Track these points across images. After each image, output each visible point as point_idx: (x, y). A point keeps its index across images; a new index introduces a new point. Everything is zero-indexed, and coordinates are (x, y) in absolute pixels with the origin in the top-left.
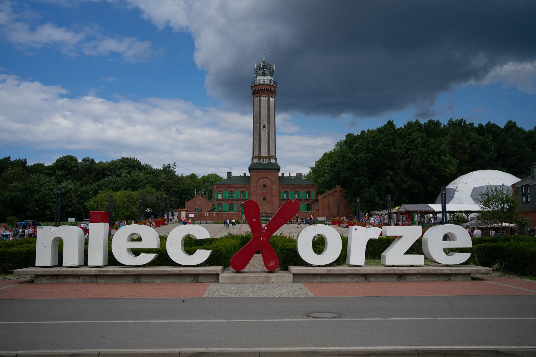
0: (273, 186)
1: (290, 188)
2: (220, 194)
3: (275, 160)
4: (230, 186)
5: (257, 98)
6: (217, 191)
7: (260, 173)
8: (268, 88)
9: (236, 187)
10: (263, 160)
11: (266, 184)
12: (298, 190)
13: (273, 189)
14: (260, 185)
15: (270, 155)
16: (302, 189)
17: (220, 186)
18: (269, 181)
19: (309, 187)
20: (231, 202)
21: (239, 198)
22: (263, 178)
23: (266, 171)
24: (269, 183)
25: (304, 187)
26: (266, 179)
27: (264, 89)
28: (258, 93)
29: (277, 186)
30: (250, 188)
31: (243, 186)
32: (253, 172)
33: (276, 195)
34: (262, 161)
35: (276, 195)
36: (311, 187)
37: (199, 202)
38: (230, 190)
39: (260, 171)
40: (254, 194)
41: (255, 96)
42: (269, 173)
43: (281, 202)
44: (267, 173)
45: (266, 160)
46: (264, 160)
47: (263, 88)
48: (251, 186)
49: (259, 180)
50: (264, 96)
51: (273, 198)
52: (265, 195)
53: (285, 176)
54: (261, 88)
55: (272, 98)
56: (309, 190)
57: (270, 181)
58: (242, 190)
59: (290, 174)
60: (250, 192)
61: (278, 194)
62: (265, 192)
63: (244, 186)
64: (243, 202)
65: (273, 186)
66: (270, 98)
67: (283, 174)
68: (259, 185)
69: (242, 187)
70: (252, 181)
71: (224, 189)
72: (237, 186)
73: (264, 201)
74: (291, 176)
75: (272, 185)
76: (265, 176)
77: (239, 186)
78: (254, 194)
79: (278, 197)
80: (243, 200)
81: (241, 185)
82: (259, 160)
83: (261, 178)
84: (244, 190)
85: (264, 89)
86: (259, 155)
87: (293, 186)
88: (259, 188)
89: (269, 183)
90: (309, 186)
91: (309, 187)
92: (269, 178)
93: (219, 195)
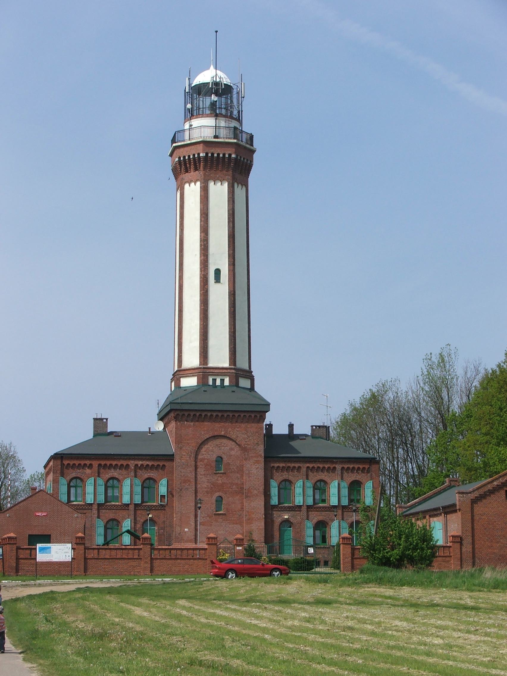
2: (75, 487)
4: (108, 463)
5: (193, 184)
6: (69, 478)
8: (229, 152)
9: (127, 465)
10: (214, 380)
14: (206, 461)
15: (235, 364)
17: (77, 462)
18: (232, 449)
20: (111, 515)
24: (233, 453)
26: (224, 441)
27: (215, 155)
28: (196, 169)
29: (257, 462)
31: (150, 463)
33: (255, 492)
34: (211, 383)
35: (255, 492)
37: (42, 512)
38: (108, 476)
41: (187, 176)
46: (218, 383)
47: (213, 154)
50: (218, 179)
53: (275, 431)
54: (207, 154)
55: (240, 186)
57: (237, 448)
58: (146, 476)
59: (291, 426)
61: (262, 488)
62: (220, 482)
63: (156, 463)
66: (236, 185)
67: (270, 426)
69: (148, 465)
71: (88, 471)
72: (132, 462)
74: (296, 432)
76: (223, 433)
80: (150, 509)
82: (203, 381)
83: (208, 437)
84: (152, 474)
85: (215, 155)
86: (200, 365)
87: (308, 465)
88: (201, 471)
89: (233, 453)
92: (233, 437)
93: (73, 490)
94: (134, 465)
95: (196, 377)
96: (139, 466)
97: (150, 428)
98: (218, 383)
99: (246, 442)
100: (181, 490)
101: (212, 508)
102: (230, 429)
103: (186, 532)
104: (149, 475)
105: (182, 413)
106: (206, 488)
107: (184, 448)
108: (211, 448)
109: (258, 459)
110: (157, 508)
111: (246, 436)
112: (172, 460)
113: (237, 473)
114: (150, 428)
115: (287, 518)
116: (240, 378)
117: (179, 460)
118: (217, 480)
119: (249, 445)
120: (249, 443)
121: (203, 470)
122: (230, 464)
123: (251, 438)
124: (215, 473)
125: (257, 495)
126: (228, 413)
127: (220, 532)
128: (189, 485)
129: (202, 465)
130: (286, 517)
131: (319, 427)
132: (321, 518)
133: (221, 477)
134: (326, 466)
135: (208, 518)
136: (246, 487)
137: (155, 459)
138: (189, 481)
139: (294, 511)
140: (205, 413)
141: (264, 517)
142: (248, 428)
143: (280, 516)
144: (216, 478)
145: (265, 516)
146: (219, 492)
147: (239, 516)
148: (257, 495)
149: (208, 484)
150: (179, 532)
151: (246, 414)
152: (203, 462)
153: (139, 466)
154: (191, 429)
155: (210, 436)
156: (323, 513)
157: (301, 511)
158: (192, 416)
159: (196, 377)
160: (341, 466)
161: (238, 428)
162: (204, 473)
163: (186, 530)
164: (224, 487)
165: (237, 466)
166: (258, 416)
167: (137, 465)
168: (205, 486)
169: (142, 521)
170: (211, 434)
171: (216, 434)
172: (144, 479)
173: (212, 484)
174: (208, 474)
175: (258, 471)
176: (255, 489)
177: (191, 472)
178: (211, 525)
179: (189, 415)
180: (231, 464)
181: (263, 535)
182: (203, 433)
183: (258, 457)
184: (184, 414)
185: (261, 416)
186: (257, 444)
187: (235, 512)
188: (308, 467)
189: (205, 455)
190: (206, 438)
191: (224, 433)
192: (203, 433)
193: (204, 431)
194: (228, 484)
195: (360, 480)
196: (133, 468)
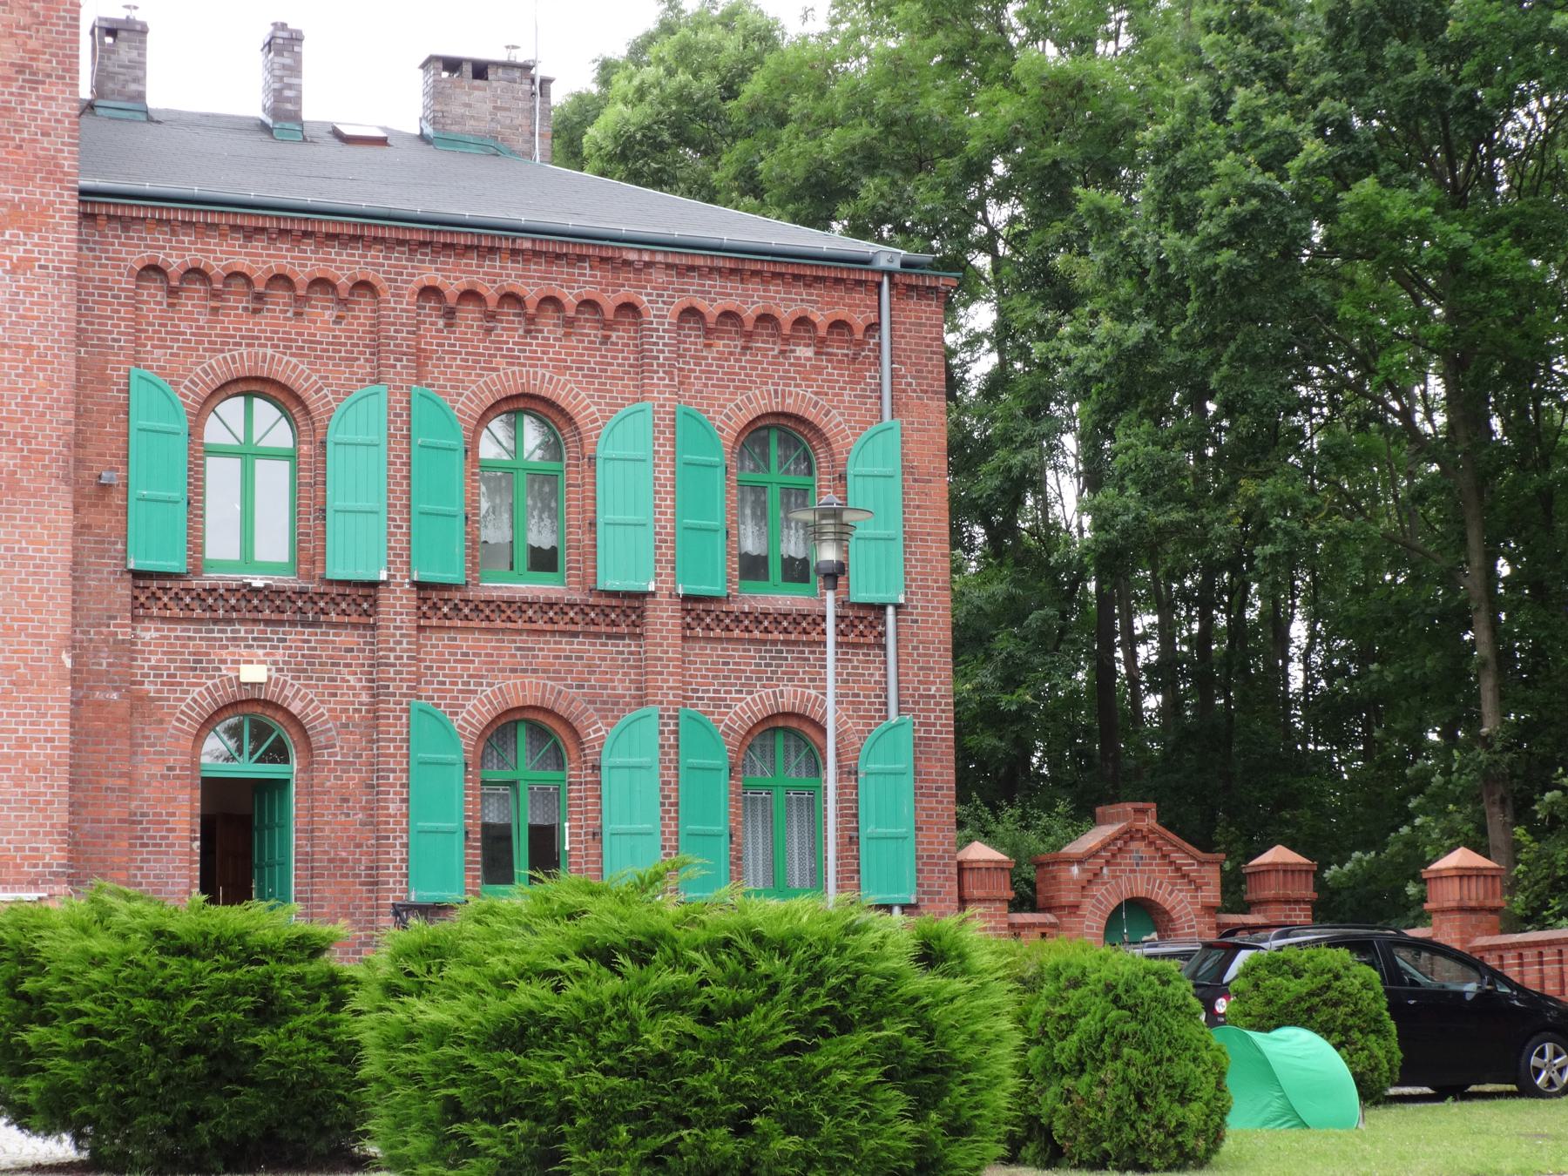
1: (363, 309)
12: (543, 381)
16: (642, 363)
19: (802, 322)
25: (691, 314)
36: (839, 325)
43: (128, 649)
56: (799, 399)
61: (54, 428)
79: (59, 511)
87: (430, 272)
90: (787, 303)
91: (802, 322)
109: (36, 192)
130: (253, 673)
131: (481, 70)
132: (524, 690)
134: (570, 297)
139: (315, 624)
141: (68, 663)
145: (74, 658)
156: (547, 649)
157: (373, 627)
160: (680, 302)
175: (29, 291)
181: (61, 816)
186: (21, 69)
188: (429, 292)
195: (811, 414)
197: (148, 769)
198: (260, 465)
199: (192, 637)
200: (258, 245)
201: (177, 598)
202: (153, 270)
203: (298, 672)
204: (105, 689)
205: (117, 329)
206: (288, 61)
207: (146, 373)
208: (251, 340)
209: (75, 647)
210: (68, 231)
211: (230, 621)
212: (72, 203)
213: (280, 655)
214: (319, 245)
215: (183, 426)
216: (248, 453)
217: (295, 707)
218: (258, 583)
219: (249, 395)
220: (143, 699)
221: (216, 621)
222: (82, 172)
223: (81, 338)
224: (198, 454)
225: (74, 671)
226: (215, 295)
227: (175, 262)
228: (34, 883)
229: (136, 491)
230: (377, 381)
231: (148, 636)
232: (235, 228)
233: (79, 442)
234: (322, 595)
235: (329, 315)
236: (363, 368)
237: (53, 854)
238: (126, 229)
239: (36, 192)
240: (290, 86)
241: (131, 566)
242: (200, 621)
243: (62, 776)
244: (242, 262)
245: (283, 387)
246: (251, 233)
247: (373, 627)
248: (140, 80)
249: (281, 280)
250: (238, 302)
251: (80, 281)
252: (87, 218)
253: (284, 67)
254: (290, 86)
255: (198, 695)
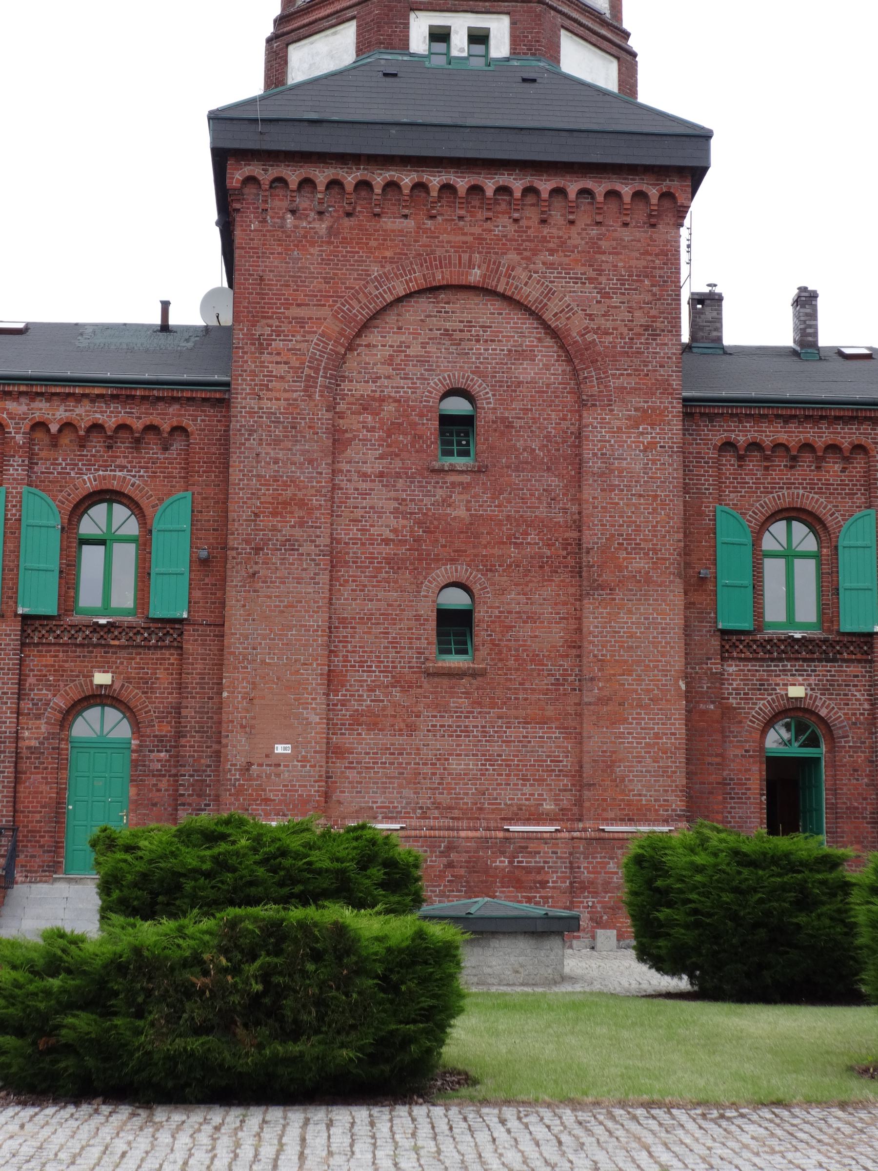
0: (588, 418)
1: (859, 464)
3: (614, 65)
7: (390, 223)
10: (440, 36)
11: (478, 387)
13: (594, 465)
14: (389, 408)
18: (520, 355)
21: (50, 609)
22: (433, 290)
23: (490, 186)
24: (526, 371)
30: (225, 442)
32: (279, 203)
33: (639, 563)
39: (392, 186)
40: (290, 544)
42: (531, 216)
43: (719, 678)
44: (503, 226)
45: (479, 38)
46: (459, 43)
48: (240, 420)
49: (366, 326)
51: (592, 623)
52: (461, 572)
58: (89, 481)
60: (223, 503)
62: (461, 512)
64: (102, 678)
65: (588, 418)
68: (366, 406)
69: (96, 427)
70: (262, 344)
73: (454, 661)
75: (582, 403)
76: (475, 276)
77: (41, 409)
78: (290, 544)
79: (675, 596)
81: (79, 398)
89: (526, 371)
92: (531, 293)
94: (25, 426)
95: (353, 25)
96: (54, 428)
97: (165, 305)
98: (459, 43)
99: (591, 317)
100: (258, 550)
101: (415, 645)
102: (513, 256)
103: (277, 763)
104: (104, 478)
105: (274, 172)
106: (387, 541)
107: (278, 344)
108: (415, 350)
109: (656, 401)
110: (139, 638)
111: (590, 292)
112: (228, 407)
113: (549, 469)
114: (165, 305)
115: (802, 695)
116: (563, 33)
117: (254, 403)
118: (446, 502)
119: (607, 333)
120: (609, 325)
121: (371, 455)
122: (510, 426)
123: (615, 300)
124: (433, 471)
125: (648, 581)
126: (504, 179)
127: (456, 765)
128: (302, 524)
129: (372, 430)
130: (796, 691)
133: (466, 487)
135: (396, 693)
136: (592, 537)
137: (133, 397)
138: (302, 504)
139: (834, 660)
140: (391, 174)
141: (683, 687)
142: (604, 253)
143: (762, 687)
144: (440, 493)
145: (687, 684)
146: (453, 561)
147: (557, 683)
148: (648, 581)
149: (393, 523)
150: (241, 761)
151: (589, 184)
152: (375, 414)
153: (54, 428)
154: (315, 250)
155: (414, 288)
157: (871, 662)
158: (321, 187)
159: (353, 25)
161: (552, 252)
162: (379, 466)
163: (280, 749)
164: (477, 536)
165: (548, 437)
166: (654, 193)
167: (40, 426)
168: (388, 534)
169: (60, 702)
170: (417, 278)
171: (440, 277)
172: (76, 497)
173: (420, 523)
174: (398, 475)
175: (654, 462)
176: (637, 548)
177: (311, 462)
178: (412, 728)
179: (307, 183)
180: (517, 423)
181: (681, 780)
182: (376, 271)
183: (650, 393)
184: (280, 181)
185: (667, 196)
187: (535, 659)
189: (386, 382)
190: (389, 298)
191: (484, 276)
192: (376, 271)
193: (382, 262)
194: (500, 524)
196: (20, 439)
197: (733, 752)
198: (798, 562)
199: (759, 670)
200: (792, 426)
201: (748, 646)
202: (728, 446)
203: (824, 690)
204: (705, 703)
205: (708, 483)
206: (808, 311)
207: (726, 508)
208: (789, 485)
209: (689, 678)
210: (677, 425)
211: (781, 660)
212: (679, 407)
213: (813, 680)
214: (830, 424)
215: (748, 540)
216: (789, 555)
217: (823, 712)
218: (798, 636)
219: (789, 520)
220: (730, 708)
221: (772, 660)
222: (684, 388)
223: (686, 488)
224: (758, 557)
225: (687, 691)
226: (767, 458)
227: (742, 439)
228: (666, 821)
229: (722, 581)
230: (869, 507)
231: (731, 669)
232: (778, 416)
233: (686, 552)
234: (838, 642)
235: (837, 467)
236: (860, 499)
237: (677, 803)
238: (711, 421)
239: (656, 401)
240: (810, 326)
241: (720, 627)
242: (762, 660)
243: (681, 756)
244: (783, 437)
245: (810, 513)
246: (787, 419)
247: (871, 662)
248: (719, 329)
249: (807, 447)
250: (781, 463)
251: (684, 453)
252: (688, 416)
253: (807, 315)
254: (810, 326)
255: (762, 705)
